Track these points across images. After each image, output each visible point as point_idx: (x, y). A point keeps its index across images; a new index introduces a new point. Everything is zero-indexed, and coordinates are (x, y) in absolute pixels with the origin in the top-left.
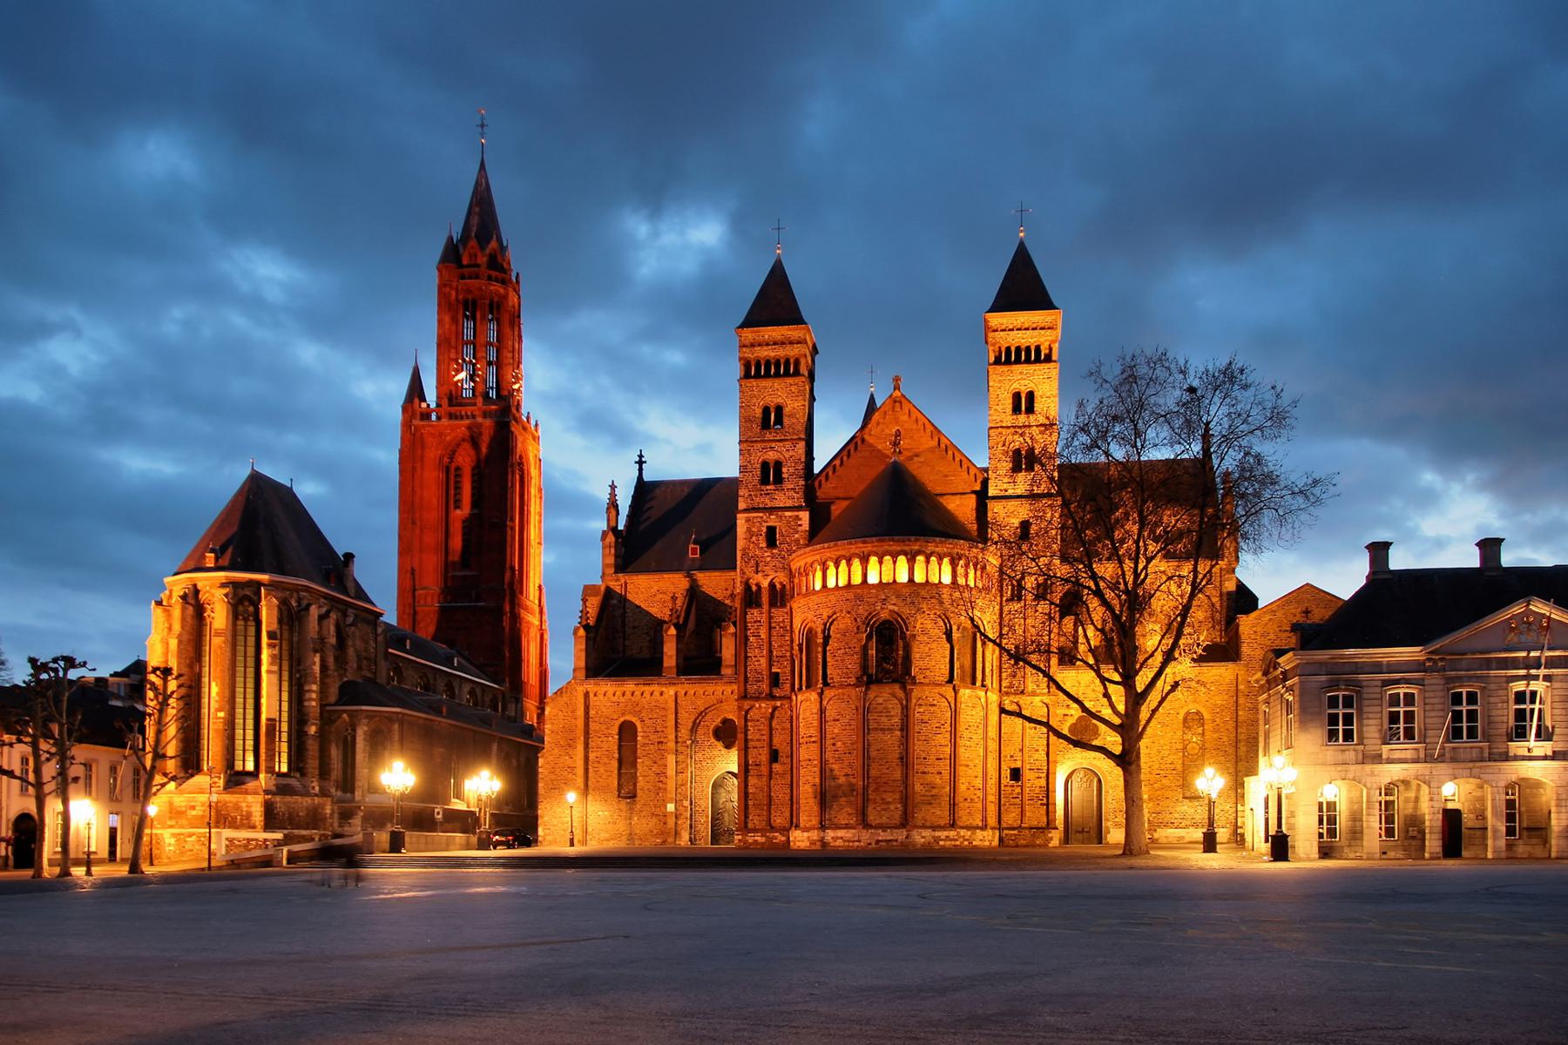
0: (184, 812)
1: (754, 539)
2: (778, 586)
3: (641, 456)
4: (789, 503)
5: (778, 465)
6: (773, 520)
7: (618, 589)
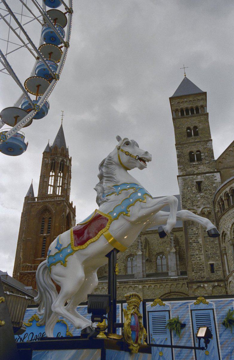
4: (207, 170)
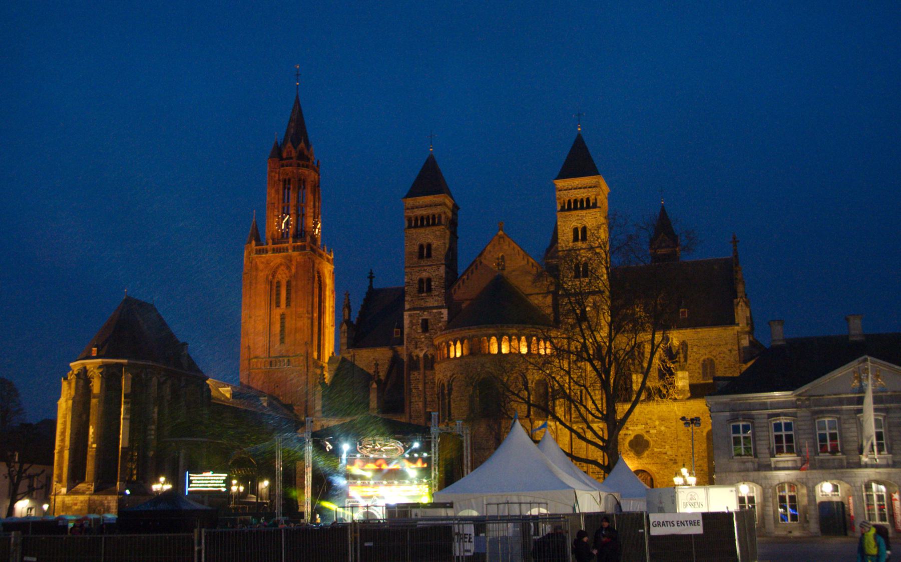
0: (71, 507)
1: (414, 327)
2: (430, 356)
3: (371, 273)
4: (436, 304)
5: (429, 280)
6: (426, 315)
7: (349, 358)
